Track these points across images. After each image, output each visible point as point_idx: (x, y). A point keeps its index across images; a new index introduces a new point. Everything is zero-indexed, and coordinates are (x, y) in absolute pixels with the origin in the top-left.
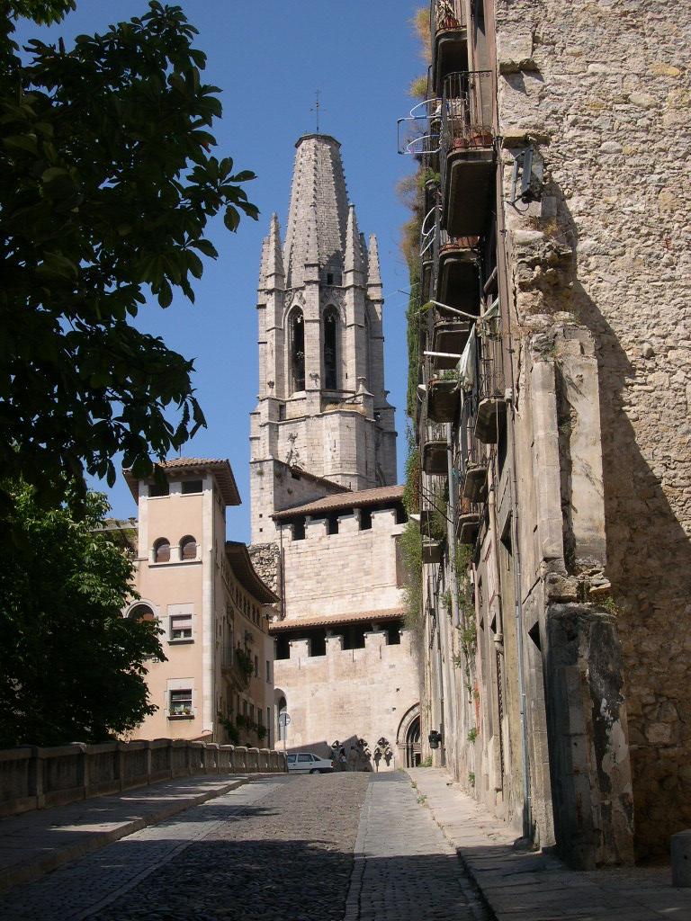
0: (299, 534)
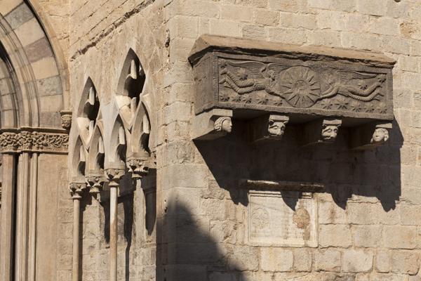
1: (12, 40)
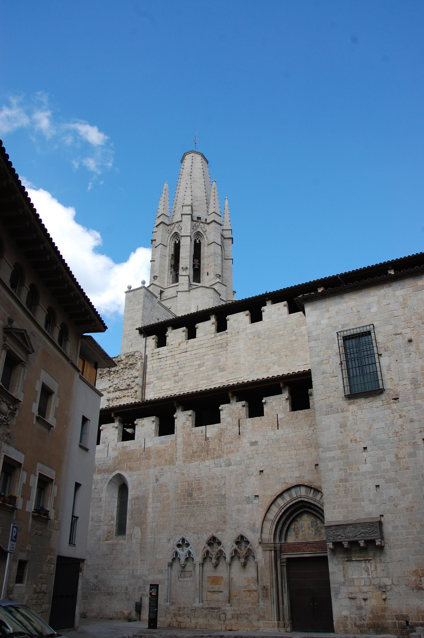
0: (162, 342)
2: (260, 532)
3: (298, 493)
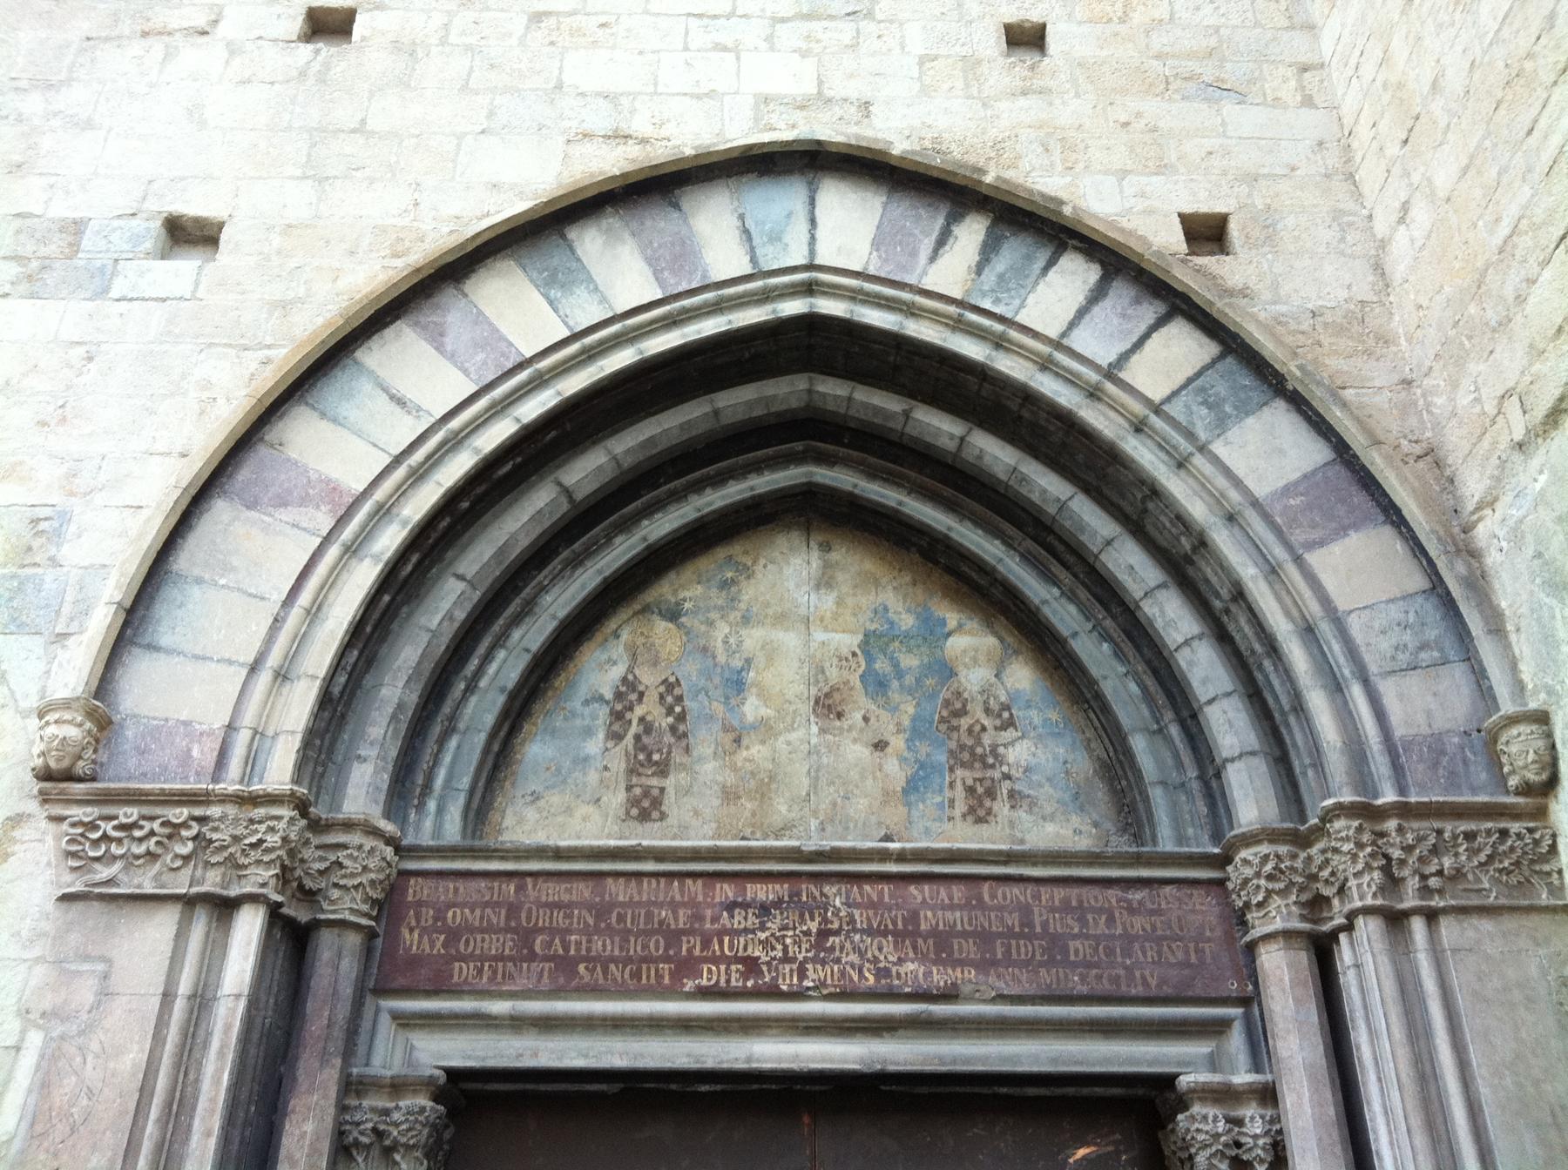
1: (1203, 485)
2: (100, 621)
3: (775, 238)
